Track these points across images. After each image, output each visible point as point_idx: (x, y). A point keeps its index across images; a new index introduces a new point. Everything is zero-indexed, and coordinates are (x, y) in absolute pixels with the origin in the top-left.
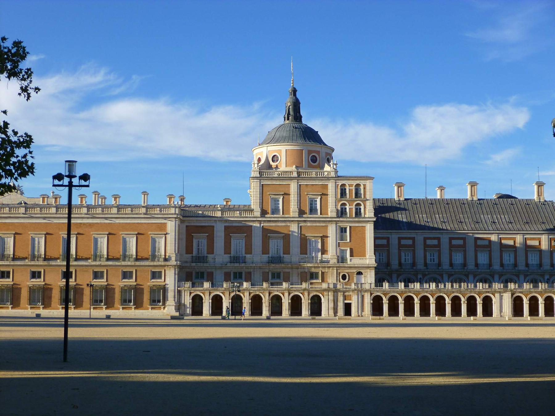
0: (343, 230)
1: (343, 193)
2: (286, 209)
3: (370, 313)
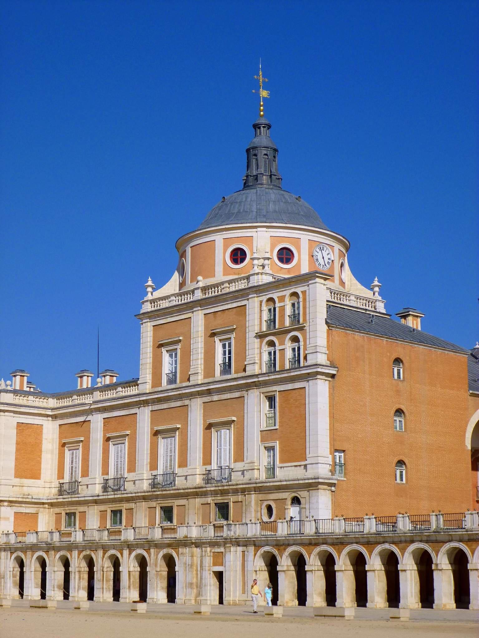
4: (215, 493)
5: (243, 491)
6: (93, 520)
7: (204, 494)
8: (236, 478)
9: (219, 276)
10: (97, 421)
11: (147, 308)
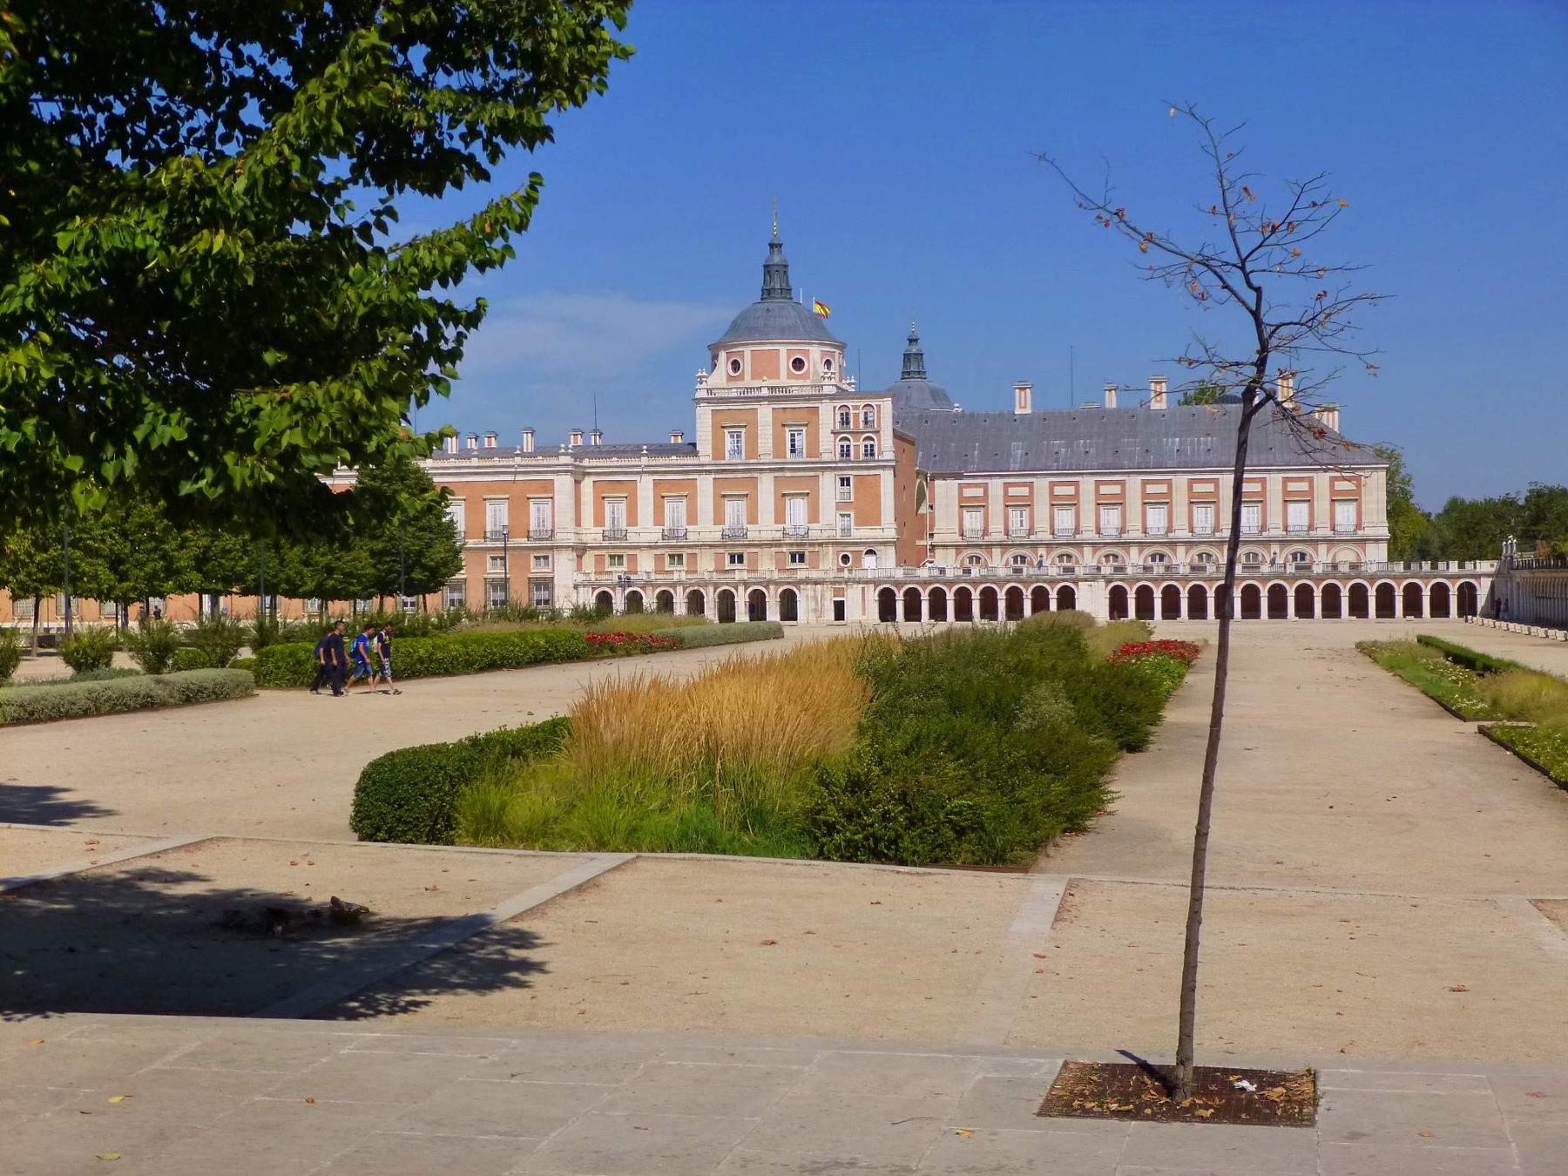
0: (845, 481)
1: (845, 420)
2: (753, 451)
3: (877, 616)
4: (791, 545)
5: (820, 545)
6: (706, 564)
7: (780, 545)
8: (814, 535)
9: (783, 380)
10: (645, 485)
11: (702, 394)
